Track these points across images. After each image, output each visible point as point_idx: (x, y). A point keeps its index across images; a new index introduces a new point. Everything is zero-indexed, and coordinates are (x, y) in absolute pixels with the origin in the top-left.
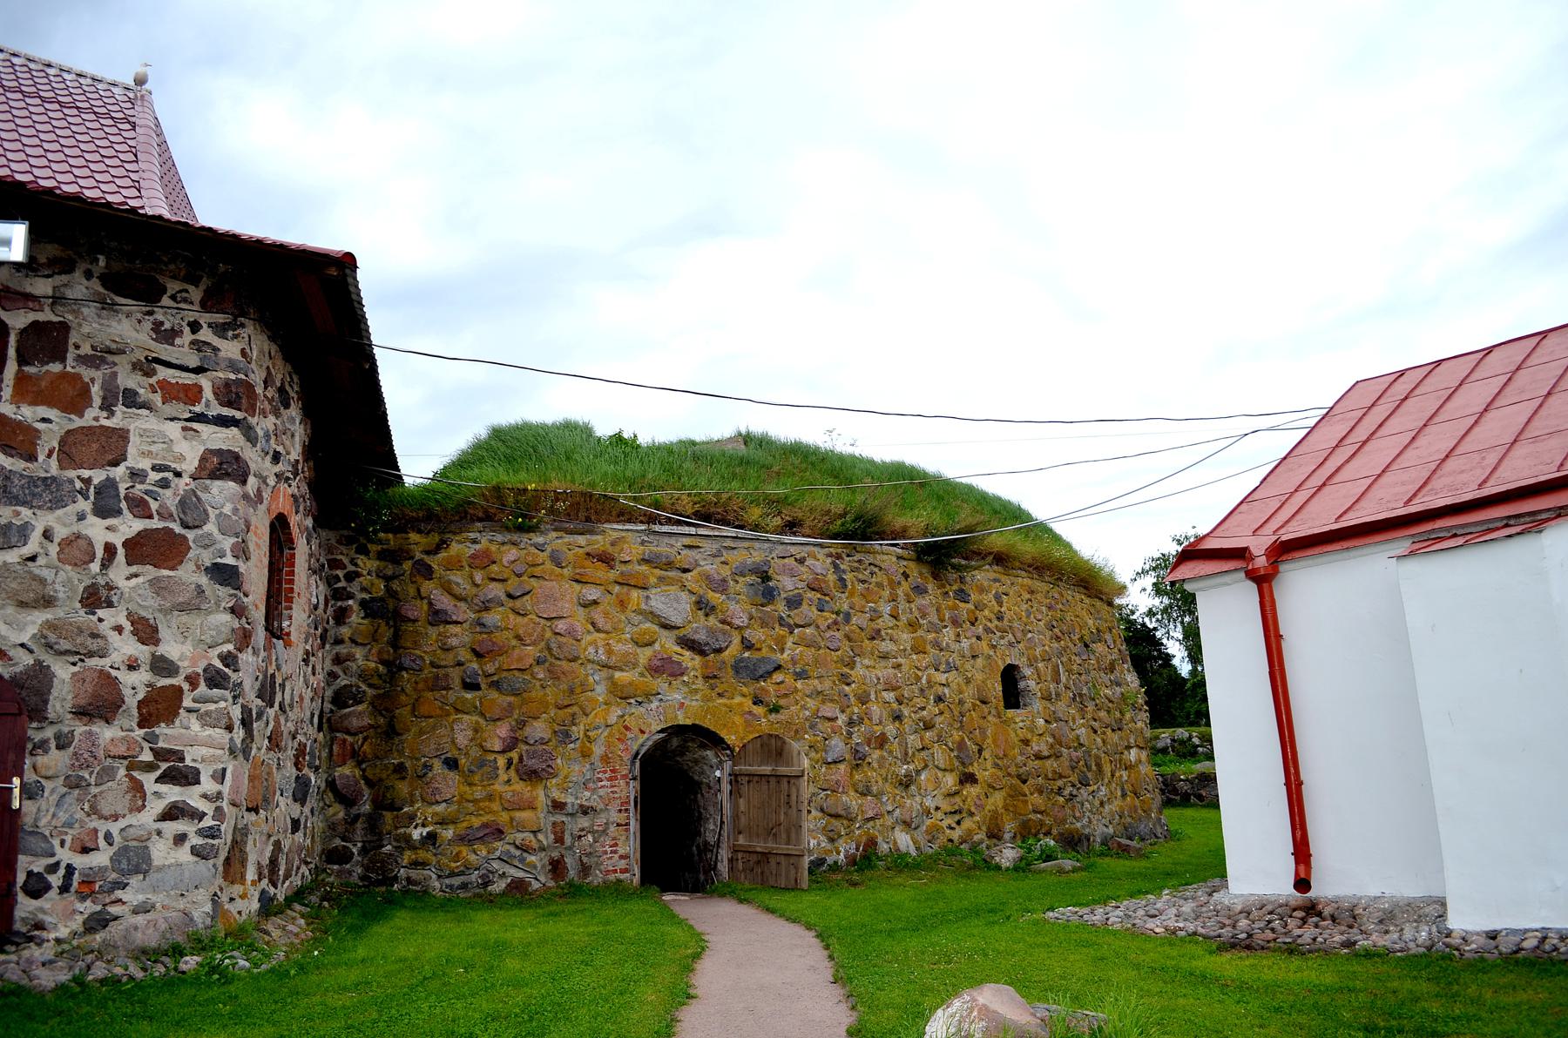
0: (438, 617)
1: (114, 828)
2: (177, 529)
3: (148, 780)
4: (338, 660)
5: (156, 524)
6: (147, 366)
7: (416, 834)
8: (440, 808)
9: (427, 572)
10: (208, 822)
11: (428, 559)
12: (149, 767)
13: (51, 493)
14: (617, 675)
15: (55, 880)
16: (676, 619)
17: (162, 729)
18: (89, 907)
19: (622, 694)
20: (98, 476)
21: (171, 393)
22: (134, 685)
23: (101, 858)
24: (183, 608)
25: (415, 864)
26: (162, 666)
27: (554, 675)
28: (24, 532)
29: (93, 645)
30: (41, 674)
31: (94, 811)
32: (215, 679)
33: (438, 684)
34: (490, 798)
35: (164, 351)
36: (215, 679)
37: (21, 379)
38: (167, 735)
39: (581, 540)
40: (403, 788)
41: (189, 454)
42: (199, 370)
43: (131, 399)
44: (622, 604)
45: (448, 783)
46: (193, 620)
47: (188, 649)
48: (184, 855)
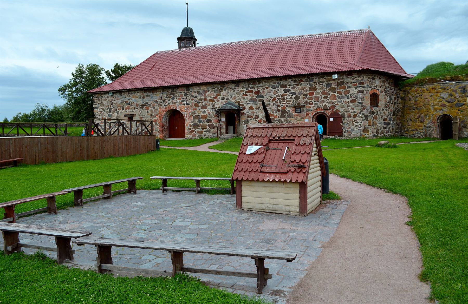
0: (410, 100)
1: (351, 127)
2: (355, 99)
3: (354, 123)
4: (398, 106)
5: (353, 99)
6: (351, 83)
7: (406, 130)
8: (410, 126)
9: (409, 93)
10: (360, 127)
11: (409, 91)
12: (354, 122)
13: (343, 97)
14: (435, 107)
15: (346, 131)
16: (445, 97)
17: (355, 118)
18: (349, 134)
19: (436, 110)
20: (347, 95)
21: (354, 85)
22: (352, 114)
23: (350, 130)
24: (356, 107)
25: (406, 134)
26: (355, 112)
28: (341, 101)
29: (348, 111)
30: (344, 114)
31: (349, 126)
32: (360, 113)
33: (410, 109)
34: (416, 125)
35: (353, 81)
36: (360, 113)
37: (340, 87)
38: (356, 119)
39: (431, 86)
40: (405, 123)
41: (356, 91)
42: (356, 82)
43: (350, 87)
44: (437, 96)
45: (410, 123)
46: (358, 107)
47: (357, 110)
48: (357, 130)
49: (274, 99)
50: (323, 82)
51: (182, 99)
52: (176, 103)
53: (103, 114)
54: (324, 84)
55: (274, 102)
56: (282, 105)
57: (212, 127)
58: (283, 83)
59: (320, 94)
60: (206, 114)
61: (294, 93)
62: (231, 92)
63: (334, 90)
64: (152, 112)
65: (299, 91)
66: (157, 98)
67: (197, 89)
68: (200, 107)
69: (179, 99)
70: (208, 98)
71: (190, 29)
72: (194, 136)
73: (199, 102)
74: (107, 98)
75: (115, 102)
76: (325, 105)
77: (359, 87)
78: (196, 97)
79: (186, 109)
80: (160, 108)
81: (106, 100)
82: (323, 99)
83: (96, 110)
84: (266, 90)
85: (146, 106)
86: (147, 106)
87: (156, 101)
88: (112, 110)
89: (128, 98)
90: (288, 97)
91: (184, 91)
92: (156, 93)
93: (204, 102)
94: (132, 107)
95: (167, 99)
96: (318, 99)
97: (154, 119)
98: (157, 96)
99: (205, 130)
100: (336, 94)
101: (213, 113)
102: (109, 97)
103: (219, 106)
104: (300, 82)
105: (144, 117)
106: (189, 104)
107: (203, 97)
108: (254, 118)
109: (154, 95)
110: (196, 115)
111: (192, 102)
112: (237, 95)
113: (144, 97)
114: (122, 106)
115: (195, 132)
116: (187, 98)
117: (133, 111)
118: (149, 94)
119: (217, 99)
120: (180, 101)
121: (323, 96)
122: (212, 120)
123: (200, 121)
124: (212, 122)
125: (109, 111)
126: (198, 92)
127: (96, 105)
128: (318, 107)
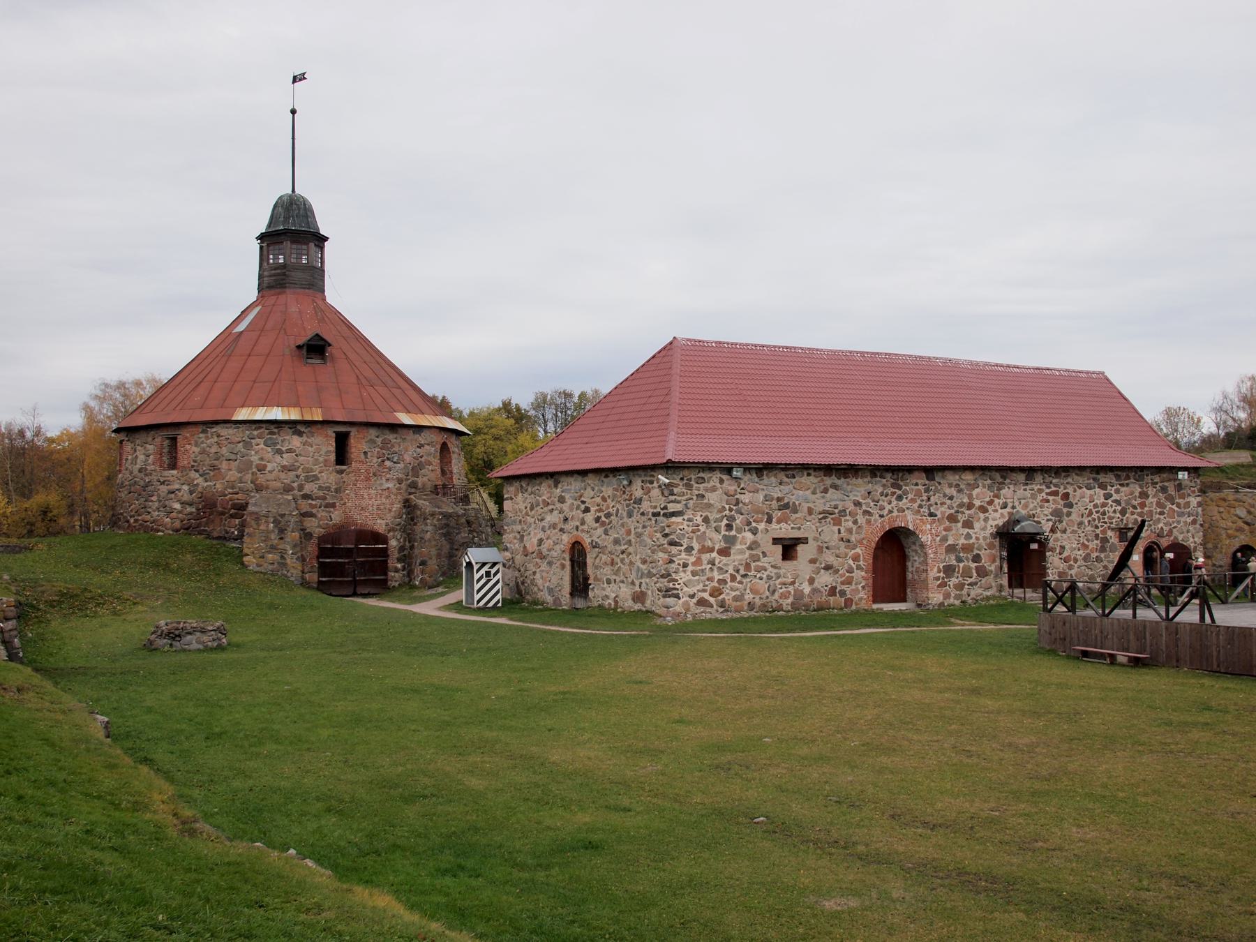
16: (1243, 516)
19: (1229, 537)
26: (1195, 543)
27: (1213, 531)
39: (1217, 494)
44: (1229, 512)
49: (1090, 513)
50: (1157, 483)
52: (906, 512)
53: (704, 533)
54: (1157, 486)
55: (1090, 518)
56: (1102, 526)
57: (982, 572)
58: (1102, 478)
59: (1154, 506)
60: (971, 541)
61: (1118, 502)
62: (1020, 492)
63: (1171, 499)
64: (850, 531)
65: (1125, 498)
66: (858, 494)
67: (952, 478)
68: (960, 525)
69: (913, 501)
70: (977, 503)
71: (305, 209)
72: (947, 596)
73: (957, 512)
74: (718, 485)
75: (746, 498)
76: (1162, 528)
77: (1199, 496)
78: (951, 498)
79: (929, 527)
80: (868, 522)
81: (714, 489)
82: (1158, 516)
83: (679, 519)
84: (1079, 492)
85: (833, 516)
86: (837, 515)
87: (857, 504)
88: (738, 521)
89: (786, 489)
90: (1110, 509)
91: (921, 479)
92: (854, 481)
93: (967, 512)
94: (797, 515)
95: (883, 497)
96: (1152, 516)
97: (853, 552)
98: (858, 488)
99: (970, 580)
100: (1174, 507)
101: (985, 538)
102: (726, 483)
103: (996, 523)
104: (1125, 479)
105: (827, 548)
106: (936, 516)
107: (966, 500)
108: (1058, 551)
109: (848, 485)
110: (949, 542)
111: (943, 509)
112: (1031, 500)
113: (825, 491)
114: (767, 513)
116: (929, 499)
117: (799, 528)
118: (839, 482)
119: (995, 507)
120: (916, 505)
121: (1159, 510)
122: (982, 556)
123: (959, 560)
124: (983, 561)
126: (957, 485)
127: (679, 502)
128: (1151, 530)
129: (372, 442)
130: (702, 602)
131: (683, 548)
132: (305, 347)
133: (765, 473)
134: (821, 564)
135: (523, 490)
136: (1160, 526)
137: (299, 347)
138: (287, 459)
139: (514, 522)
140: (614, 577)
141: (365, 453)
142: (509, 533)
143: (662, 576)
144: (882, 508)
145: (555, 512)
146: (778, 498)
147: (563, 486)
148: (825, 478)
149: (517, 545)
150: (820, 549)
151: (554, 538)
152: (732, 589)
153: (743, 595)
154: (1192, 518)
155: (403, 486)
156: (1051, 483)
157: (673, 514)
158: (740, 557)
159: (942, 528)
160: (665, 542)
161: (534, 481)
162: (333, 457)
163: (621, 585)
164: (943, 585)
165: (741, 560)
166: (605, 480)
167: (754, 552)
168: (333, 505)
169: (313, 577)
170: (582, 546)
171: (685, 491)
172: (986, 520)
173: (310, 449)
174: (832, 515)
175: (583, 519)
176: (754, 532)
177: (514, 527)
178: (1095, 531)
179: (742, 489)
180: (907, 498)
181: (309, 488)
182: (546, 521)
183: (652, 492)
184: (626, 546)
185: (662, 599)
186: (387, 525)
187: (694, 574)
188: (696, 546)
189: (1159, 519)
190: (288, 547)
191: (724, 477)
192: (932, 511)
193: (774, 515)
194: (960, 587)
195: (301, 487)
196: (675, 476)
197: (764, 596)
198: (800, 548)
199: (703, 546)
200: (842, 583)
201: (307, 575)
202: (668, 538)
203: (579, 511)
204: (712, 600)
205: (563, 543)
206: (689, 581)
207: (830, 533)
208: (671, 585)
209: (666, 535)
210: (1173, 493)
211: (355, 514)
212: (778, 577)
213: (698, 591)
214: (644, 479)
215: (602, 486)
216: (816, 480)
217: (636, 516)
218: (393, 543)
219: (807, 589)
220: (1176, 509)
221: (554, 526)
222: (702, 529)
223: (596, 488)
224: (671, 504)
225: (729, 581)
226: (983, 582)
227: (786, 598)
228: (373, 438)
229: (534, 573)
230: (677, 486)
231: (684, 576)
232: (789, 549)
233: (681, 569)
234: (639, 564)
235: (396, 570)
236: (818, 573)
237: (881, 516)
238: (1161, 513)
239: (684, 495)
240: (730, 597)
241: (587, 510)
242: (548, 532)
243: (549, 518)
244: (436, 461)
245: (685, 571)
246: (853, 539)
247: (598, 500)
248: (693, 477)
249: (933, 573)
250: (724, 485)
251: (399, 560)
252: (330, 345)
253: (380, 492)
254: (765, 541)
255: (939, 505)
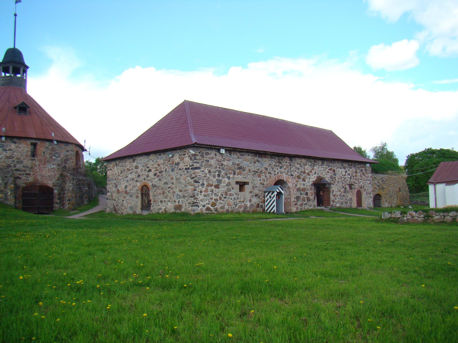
26: (370, 191)
49: (341, 178)
51: (287, 170)
52: (283, 173)
53: (209, 177)
56: (345, 183)
57: (309, 200)
63: (363, 174)
64: (264, 180)
65: (351, 173)
67: (298, 160)
68: (301, 180)
70: (307, 171)
73: (300, 175)
74: (214, 156)
75: (225, 163)
78: (298, 169)
79: (291, 180)
80: (270, 177)
81: (213, 158)
82: (360, 180)
83: (198, 171)
84: (338, 169)
85: (258, 173)
87: (266, 169)
88: (222, 173)
89: (240, 160)
92: (265, 159)
93: (304, 175)
95: (275, 167)
98: (266, 162)
100: (365, 177)
103: (313, 180)
106: (293, 176)
107: (303, 170)
112: (323, 172)
113: (255, 163)
114: (234, 170)
115: (297, 205)
117: (246, 178)
118: (260, 159)
120: (286, 171)
121: (361, 178)
123: (301, 194)
125: (218, 175)
126: (300, 164)
127: (198, 163)
129: (47, 148)
130: (208, 209)
131: (200, 184)
132: (18, 108)
133: (232, 153)
134: (254, 194)
135: (117, 165)
136: (361, 184)
137: (15, 108)
138: (9, 154)
139: (113, 179)
140: (164, 199)
141: (44, 152)
142: (110, 185)
143: (191, 197)
144: (275, 171)
145: (133, 173)
146: (237, 164)
147: (138, 161)
148: (254, 157)
149: (114, 190)
150: (253, 187)
151: (132, 185)
152: (220, 203)
153: (224, 206)
154: (369, 182)
155: (60, 167)
156: (329, 165)
157: (196, 168)
158: (223, 189)
159: (295, 181)
160: (192, 181)
161: (122, 161)
162: (29, 153)
163: (168, 203)
164: (296, 204)
165: (223, 191)
166: (160, 157)
167: (229, 187)
168: (29, 174)
169: (20, 205)
170: (147, 187)
171: (201, 158)
172: (310, 178)
173: (19, 149)
174: (257, 173)
175: (148, 175)
176: (229, 178)
177: (112, 182)
178: (342, 185)
179: (224, 159)
180: (283, 168)
181: (18, 166)
182: (129, 177)
183: (185, 159)
184: (171, 185)
185: (191, 208)
186: (53, 184)
187: (205, 196)
188: (206, 183)
189: (361, 181)
190: (8, 191)
191: (217, 153)
192: (292, 174)
193: (236, 171)
194: (301, 205)
195: (15, 166)
196: (197, 151)
197: (232, 207)
198: (246, 186)
199: (209, 183)
200: (261, 202)
201: (17, 205)
202: (194, 179)
203: (146, 172)
204: (212, 208)
205: (138, 186)
206: (203, 199)
207: (257, 181)
208: (195, 201)
209: (192, 178)
210: (364, 172)
211: (39, 178)
212: (238, 199)
213: (207, 204)
214: (180, 154)
215: (158, 159)
216: (251, 158)
217: (176, 171)
218: (56, 191)
219: (248, 204)
220: (365, 178)
221: (133, 179)
222: (208, 175)
223: (155, 161)
224: (195, 164)
225: (219, 199)
226: (309, 203)
227: (241, 208)
228: (48, 146)
229: (123, 201)
230: (197, 156)
231: (201, 197)
232: (242, 185)
233: (199, 193)
234: (178, 192)
235: (57, 203)
236: (253, 198)
237: (275, 175)
238: (361, 179)
239: (200, 160)
240: (219, 207)
241: (150, 171)
242: (130, 182)
243: (130, 176)
244: (74, 158)
245: (201, 195)
246: (265, 184)
247: (156, 166)
248: (204, 152)
249: (293, 199)
250: (217, 157)
251: (58, 199)
252: (29, 107)
253: (50, 169)
254: (233, 182)
255: (294, 172)
